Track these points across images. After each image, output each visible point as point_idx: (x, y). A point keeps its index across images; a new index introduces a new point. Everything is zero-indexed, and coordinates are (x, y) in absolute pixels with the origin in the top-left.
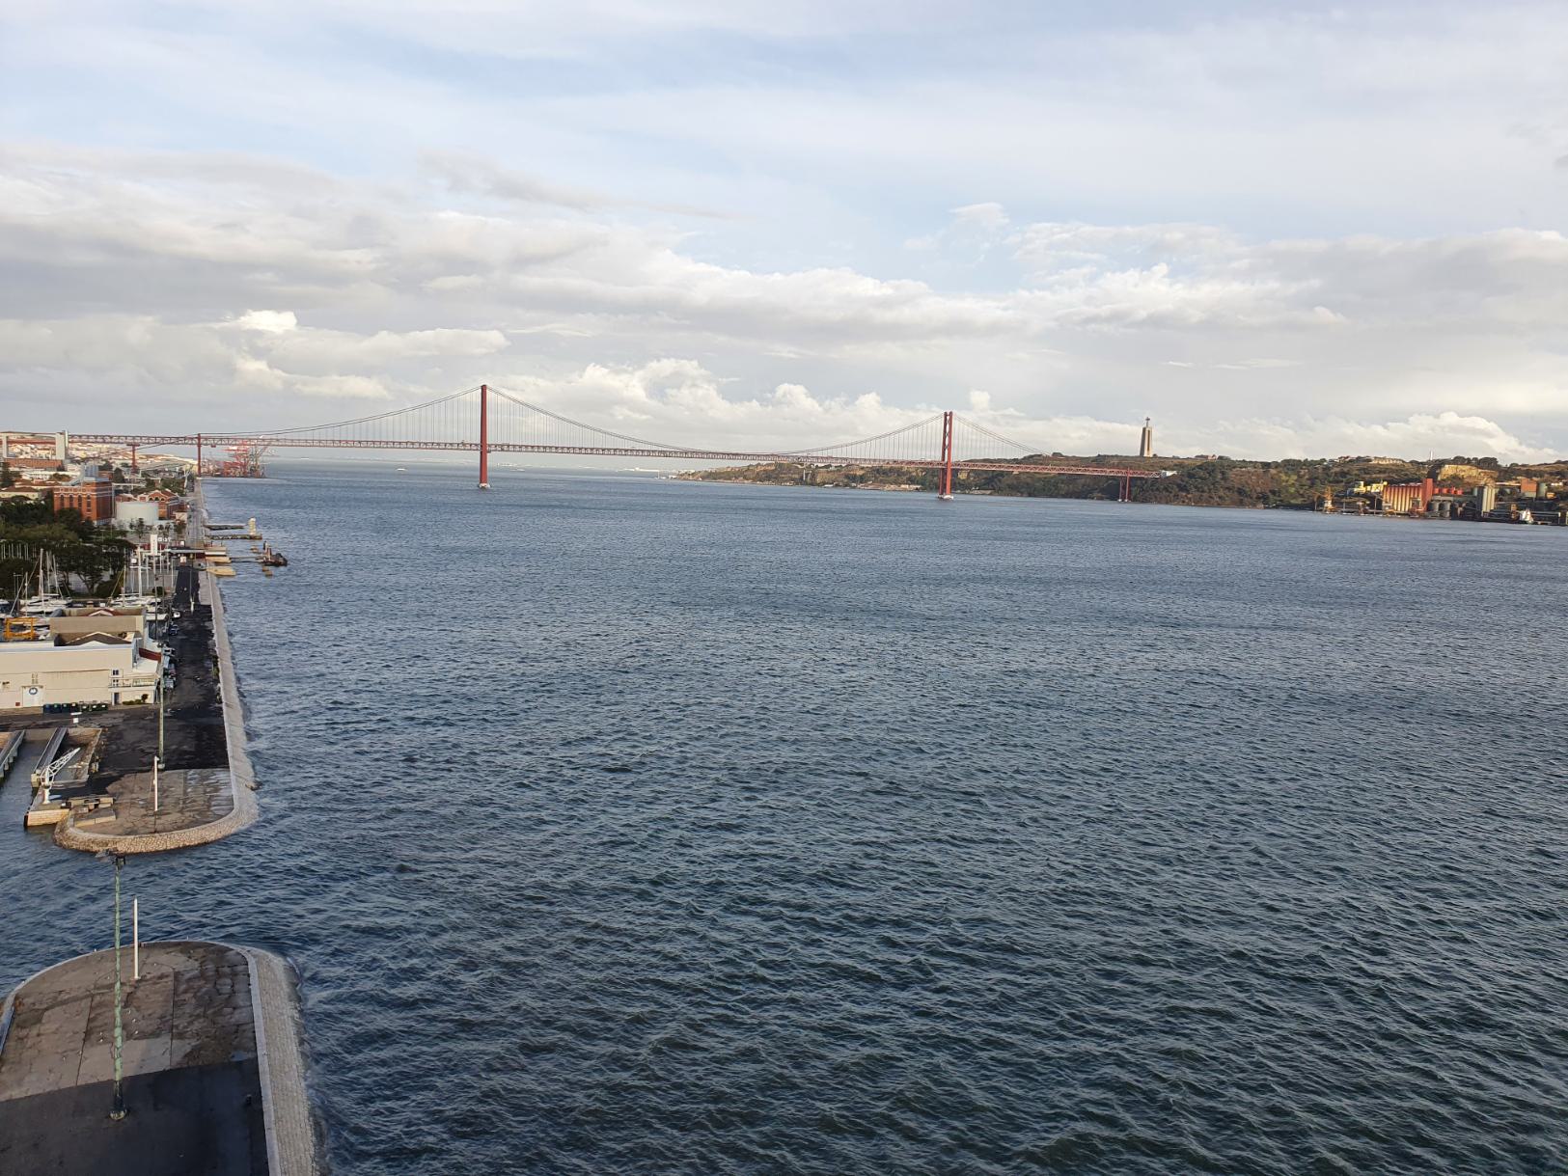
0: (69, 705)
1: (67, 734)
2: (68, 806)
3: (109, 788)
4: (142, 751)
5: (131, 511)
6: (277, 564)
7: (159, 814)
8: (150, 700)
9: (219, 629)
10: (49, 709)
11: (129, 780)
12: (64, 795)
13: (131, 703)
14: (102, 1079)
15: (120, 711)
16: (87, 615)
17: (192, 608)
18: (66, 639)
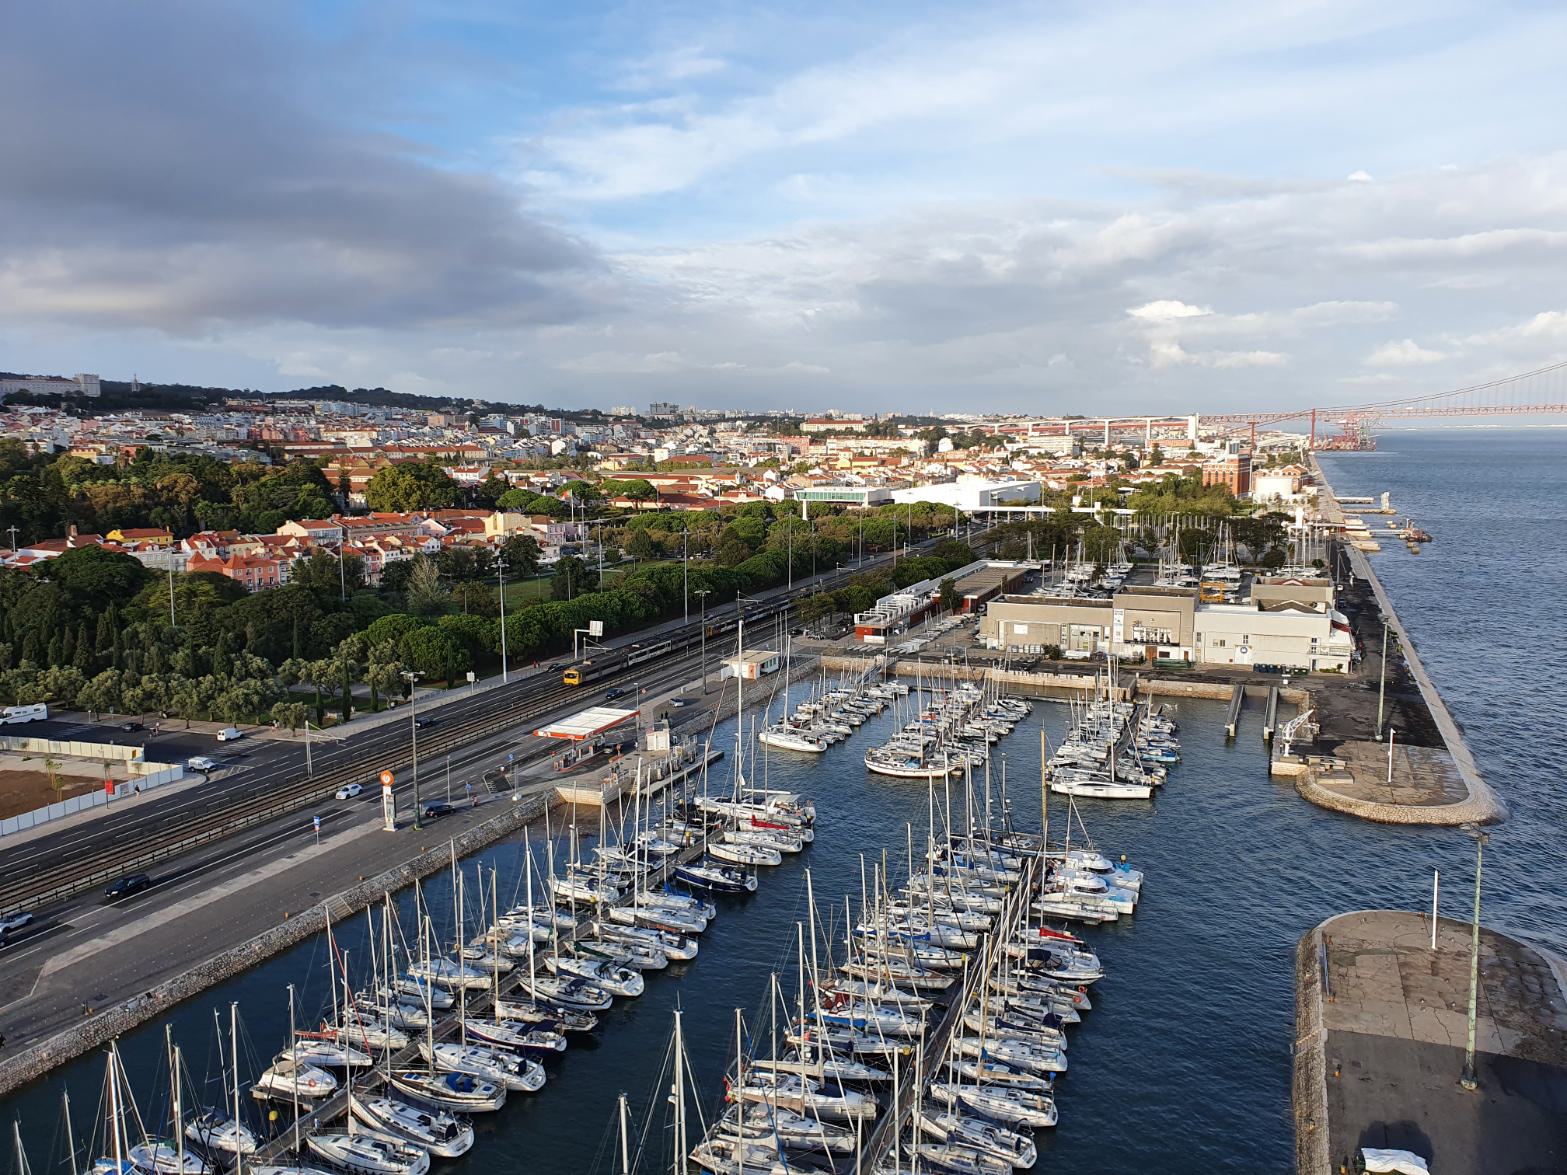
0: (1275, 667)
1: (1279, 694)
2: (1306, 762)
3: (1335, 751)
5: (1270, 488)
6: (1420, 541)
7: (1394, 785)
8: (1345, 670)
10: (1259, 668)
11: (1351, 747)
12: (1300, 750)
13: (1327, 671)
14: (1437, 1041)
15: (1320, 678)
16: (1280, 583)
18: (1264, 604)
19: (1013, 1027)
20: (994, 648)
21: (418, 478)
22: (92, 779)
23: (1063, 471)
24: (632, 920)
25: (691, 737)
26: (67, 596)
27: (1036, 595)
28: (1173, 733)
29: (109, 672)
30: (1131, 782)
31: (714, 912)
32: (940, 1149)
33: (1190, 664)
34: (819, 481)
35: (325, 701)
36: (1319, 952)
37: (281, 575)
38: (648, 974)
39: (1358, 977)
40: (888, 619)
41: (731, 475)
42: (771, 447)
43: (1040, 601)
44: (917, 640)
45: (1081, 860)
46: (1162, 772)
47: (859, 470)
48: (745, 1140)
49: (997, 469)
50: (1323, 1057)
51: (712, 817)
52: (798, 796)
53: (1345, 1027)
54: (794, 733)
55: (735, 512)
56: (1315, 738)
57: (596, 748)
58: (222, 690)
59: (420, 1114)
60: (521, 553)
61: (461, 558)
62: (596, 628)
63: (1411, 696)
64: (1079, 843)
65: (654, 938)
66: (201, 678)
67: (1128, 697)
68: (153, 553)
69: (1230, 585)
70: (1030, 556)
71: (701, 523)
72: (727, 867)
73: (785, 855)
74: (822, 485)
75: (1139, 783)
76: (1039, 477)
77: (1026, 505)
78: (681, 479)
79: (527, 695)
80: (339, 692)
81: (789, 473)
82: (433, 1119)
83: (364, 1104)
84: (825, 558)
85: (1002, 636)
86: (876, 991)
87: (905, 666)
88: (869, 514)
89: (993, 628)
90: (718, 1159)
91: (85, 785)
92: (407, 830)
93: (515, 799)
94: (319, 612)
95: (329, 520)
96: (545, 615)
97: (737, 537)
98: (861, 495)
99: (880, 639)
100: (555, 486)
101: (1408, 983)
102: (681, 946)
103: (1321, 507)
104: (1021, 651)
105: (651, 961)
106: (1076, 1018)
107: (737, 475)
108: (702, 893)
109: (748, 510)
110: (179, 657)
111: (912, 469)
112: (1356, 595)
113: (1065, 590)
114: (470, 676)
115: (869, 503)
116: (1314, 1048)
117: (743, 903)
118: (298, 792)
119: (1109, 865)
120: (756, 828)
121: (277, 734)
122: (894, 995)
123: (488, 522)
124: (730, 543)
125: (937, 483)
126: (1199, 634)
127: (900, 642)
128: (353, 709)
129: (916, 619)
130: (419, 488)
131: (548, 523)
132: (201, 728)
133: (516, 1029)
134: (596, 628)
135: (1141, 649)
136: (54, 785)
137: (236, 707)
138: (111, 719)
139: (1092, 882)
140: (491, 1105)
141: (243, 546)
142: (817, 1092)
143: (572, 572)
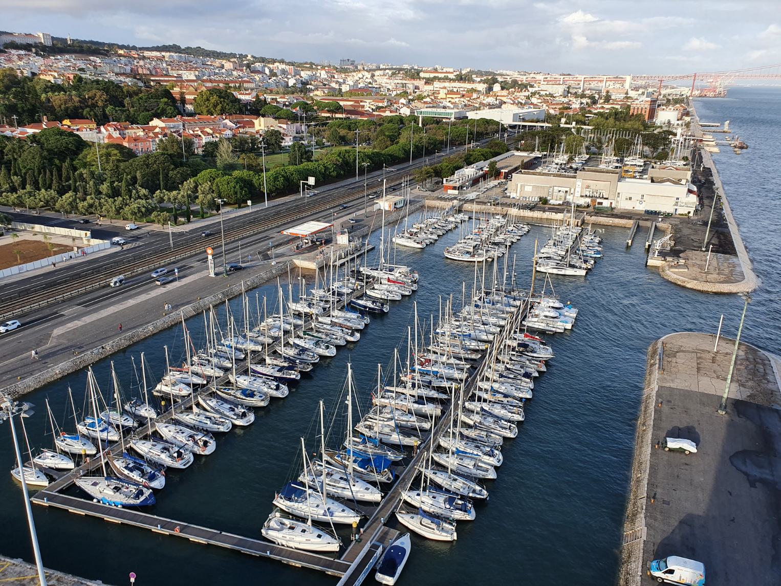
0: (656, 212)
2: (665, 260)
3: (681, 255)
4: (692, 240)
5: (666, 116)
6: (742, 148)
8: (691, 215)
9: (717, 180)
10: (647, 212)
11: (689, 253)
12: (663, 254)
13: (682, 215)
14: (710, 393)
15: (678, 218)
16: (664, 169)
17: (701, 169)
18: (654, 179)
19: (509, 378)
20: (514, 198)
21: (220, 97)
22: (67, 246)
23: (557, 104)
24: (330, 322)
25: (359, 239)
26: (45, 153)
27: (539, 170)
28: (599, 243)
29: (70, 193)
30: (577, 268)
31: (369, 321)
32: (470, 430)
33: (612, 209)
34: (429, 105)
35: (178, 212)
36: (659, 351)
37: (153, 147)
38: (338, 347)
39: (676, 363)
40: (461, 182)
41: (382, 100)
42: (404, 85)
43: (540, 174)
44: (475, 193)
45: (548, 303)
46: (592, 262)
47: (450, 99)
48: (380, 422)
49: (523, 102)
50: (654, 398)
51: (368, 277)
52: (410, 268)
53: (667, 385)
54: (410, 238)
55: (383, 121)
56: (671, 249)
57: (312, 241)
58: (126, 204)
59: (230, 406)
60: (273, 141)
61: (243, 142)
62: (312, 181)
63: (723, 229)
64: (549, 294)
65: (340, 331)
66: (116, 198)
67: (579, 224)
68: (87, 132)
69: (638, 168)
70: (536, 149)
71: (366, 126)
72: (374, 300)
73: (403, 296)
74: (430, 107)
75: (580, 268)
76: (545, 107)
77: (537, 122)
78: (356, 102)
79: (277, 213)
80: (184, 208)
81: (413, 100)
82: (236, 409)
83: (204, 400)
84: (430, 148)
85: (518, 191)
86: (444, 359)
87: (467, 206)
88: (454, 124)
89: (514, 187)
90: (367, 430)
91: (65, 249)
92: (221, 276)
93: (273, 264)
94: (173, 166)
95: (175, 119)
96: (286, 173)
97: (384, 135)
98: (451, 114)
99: (456, 192)
100: (290, 104)
101: (699, 366)
102: (352, 335)
103: (691, 128)
104: (527, 200)
105: (339, 341)
106: (536, 374)
107: (386, 100)
108: (364, 312)
109: (391, 120)
110: (104, 188)
111: (478, 100)
112: (703, 176)
113: (553, 168)
114: (249, 203)
115: (455, 118)
116: (650, 394)
117: (382, 319)
118: (167, 256)
119: (562, 305)
120: (389, 283)
121: (156, 227)
122: (452, 361)
123: (256, 122)
124: (380, 138)
125: (491, 108)
126: (619, 194)
127: (466, 193)
128: (192, 216)
129: (475, 181)
130: (221, 103)
131: (287, 124)
132: (119, 223)
133: (276, 369)
134: (312, 181)
135: (589, 200)
136: (49, 247)
137: (134, 213)
138: (73, 217)
139: (553, 314)
140: (262, 404)
141: (133, 131)
142: (414, 402)
143: (299, 150)
